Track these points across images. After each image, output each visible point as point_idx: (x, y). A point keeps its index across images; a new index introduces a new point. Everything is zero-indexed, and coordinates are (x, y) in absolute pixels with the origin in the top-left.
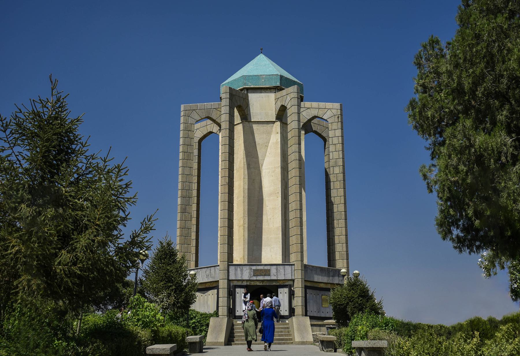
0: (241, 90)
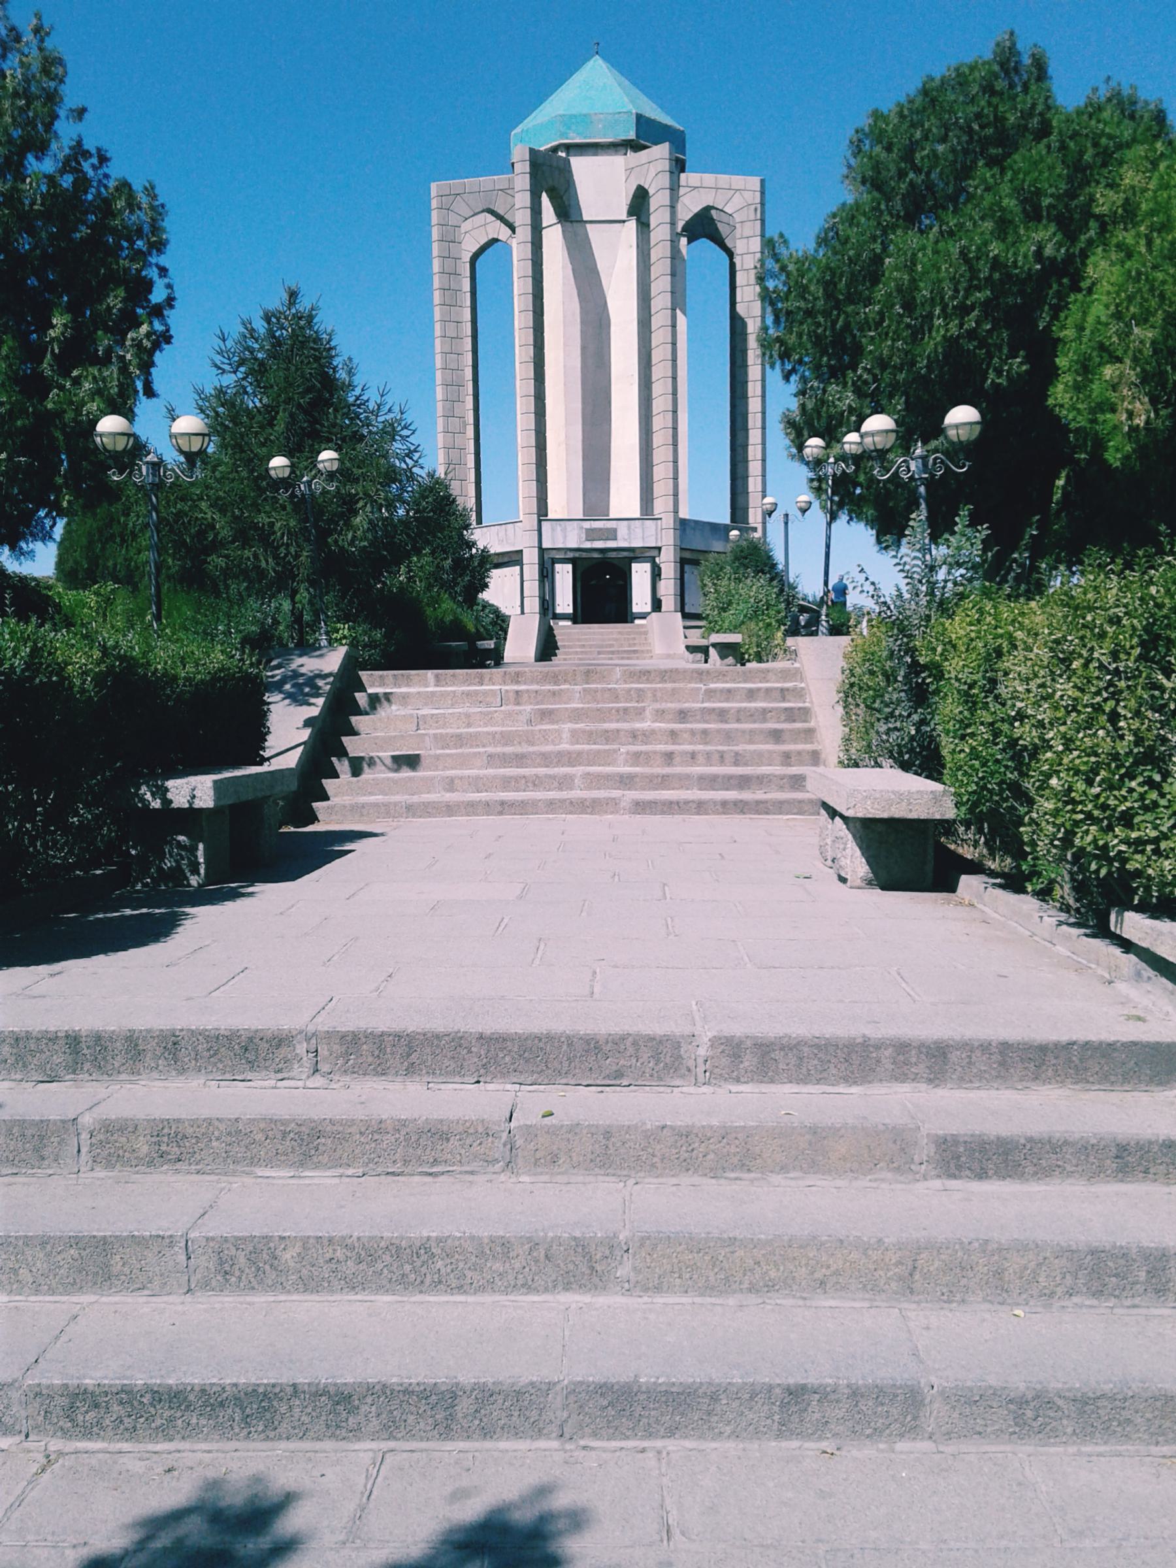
0: (555, 149)
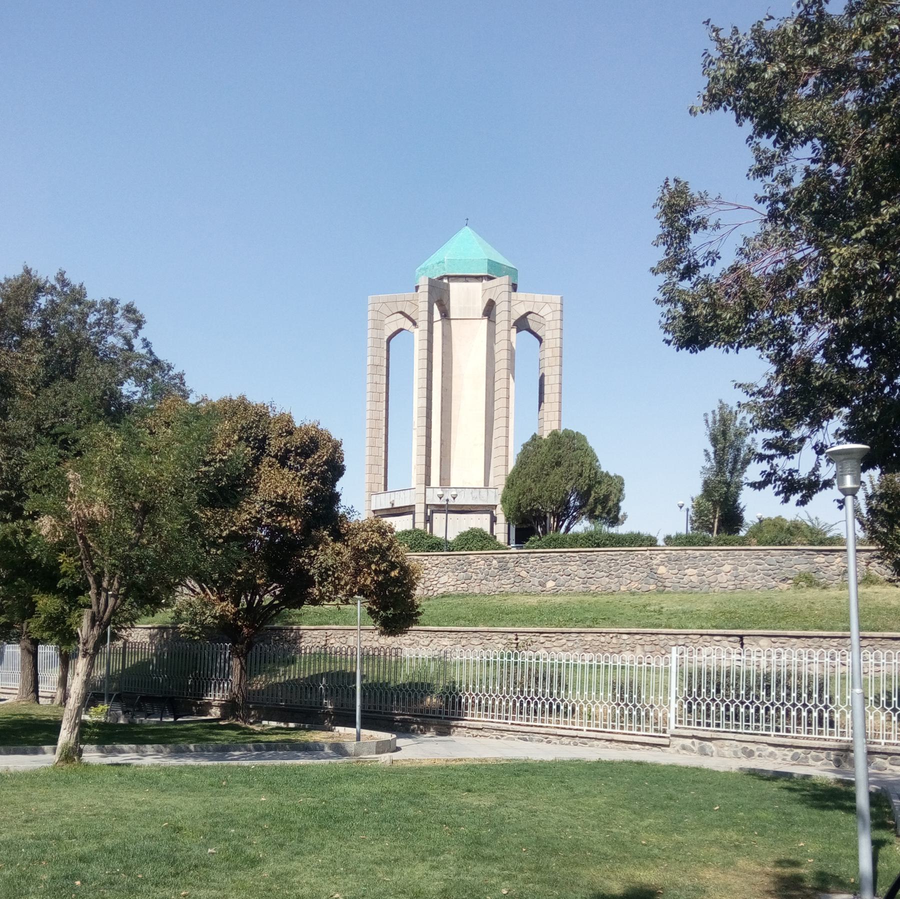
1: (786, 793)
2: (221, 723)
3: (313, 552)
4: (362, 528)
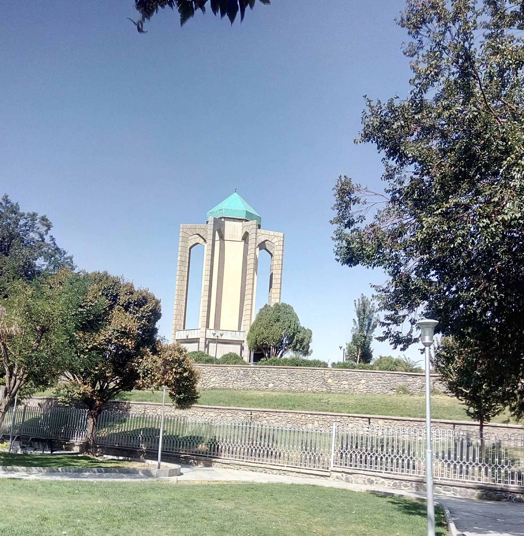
0: (221, 218)
1: (390, 504)
2: (79, 455)
3: (140, 360)
4: (169, 348)
